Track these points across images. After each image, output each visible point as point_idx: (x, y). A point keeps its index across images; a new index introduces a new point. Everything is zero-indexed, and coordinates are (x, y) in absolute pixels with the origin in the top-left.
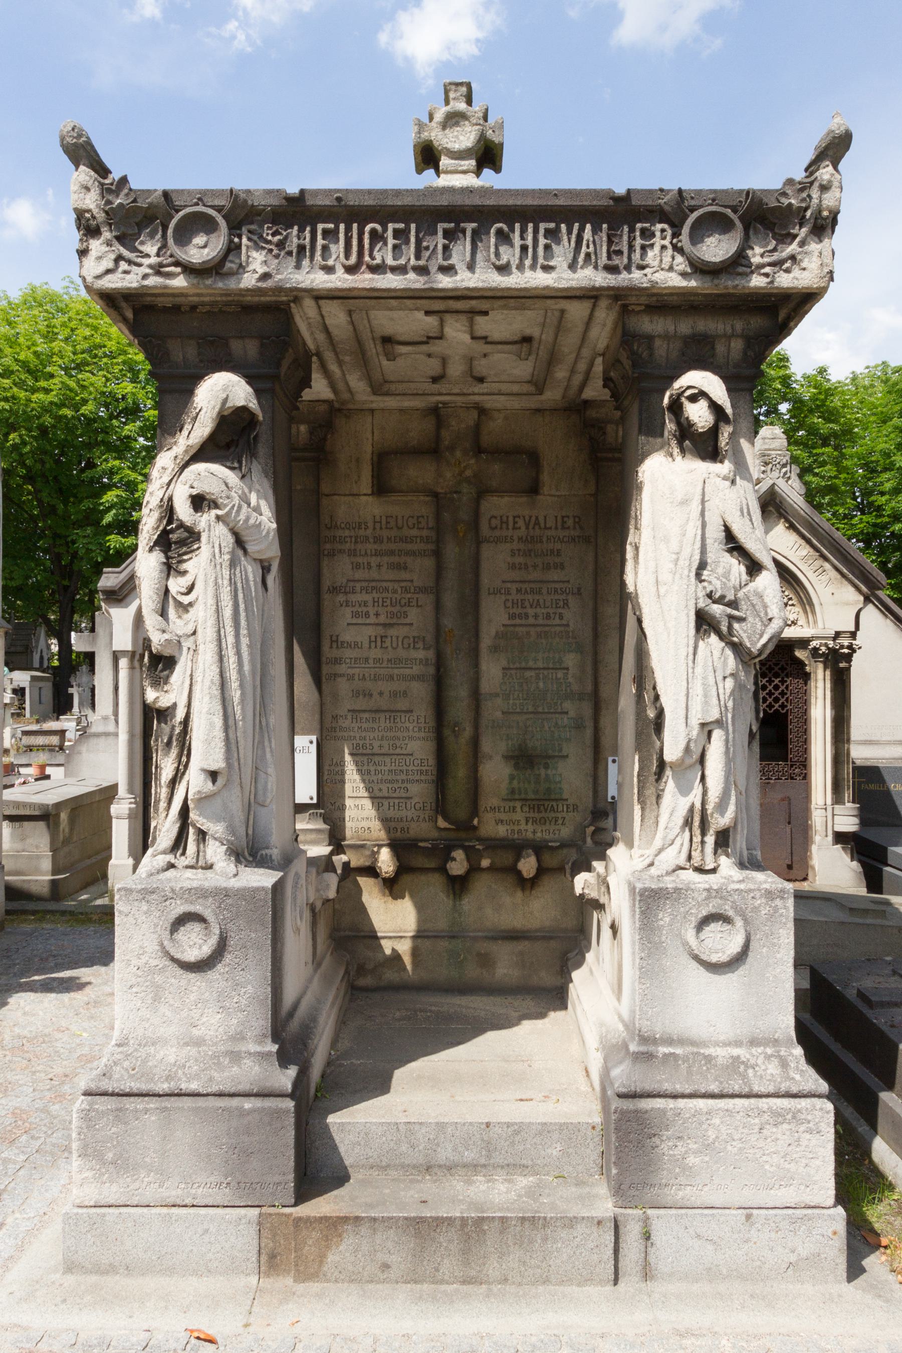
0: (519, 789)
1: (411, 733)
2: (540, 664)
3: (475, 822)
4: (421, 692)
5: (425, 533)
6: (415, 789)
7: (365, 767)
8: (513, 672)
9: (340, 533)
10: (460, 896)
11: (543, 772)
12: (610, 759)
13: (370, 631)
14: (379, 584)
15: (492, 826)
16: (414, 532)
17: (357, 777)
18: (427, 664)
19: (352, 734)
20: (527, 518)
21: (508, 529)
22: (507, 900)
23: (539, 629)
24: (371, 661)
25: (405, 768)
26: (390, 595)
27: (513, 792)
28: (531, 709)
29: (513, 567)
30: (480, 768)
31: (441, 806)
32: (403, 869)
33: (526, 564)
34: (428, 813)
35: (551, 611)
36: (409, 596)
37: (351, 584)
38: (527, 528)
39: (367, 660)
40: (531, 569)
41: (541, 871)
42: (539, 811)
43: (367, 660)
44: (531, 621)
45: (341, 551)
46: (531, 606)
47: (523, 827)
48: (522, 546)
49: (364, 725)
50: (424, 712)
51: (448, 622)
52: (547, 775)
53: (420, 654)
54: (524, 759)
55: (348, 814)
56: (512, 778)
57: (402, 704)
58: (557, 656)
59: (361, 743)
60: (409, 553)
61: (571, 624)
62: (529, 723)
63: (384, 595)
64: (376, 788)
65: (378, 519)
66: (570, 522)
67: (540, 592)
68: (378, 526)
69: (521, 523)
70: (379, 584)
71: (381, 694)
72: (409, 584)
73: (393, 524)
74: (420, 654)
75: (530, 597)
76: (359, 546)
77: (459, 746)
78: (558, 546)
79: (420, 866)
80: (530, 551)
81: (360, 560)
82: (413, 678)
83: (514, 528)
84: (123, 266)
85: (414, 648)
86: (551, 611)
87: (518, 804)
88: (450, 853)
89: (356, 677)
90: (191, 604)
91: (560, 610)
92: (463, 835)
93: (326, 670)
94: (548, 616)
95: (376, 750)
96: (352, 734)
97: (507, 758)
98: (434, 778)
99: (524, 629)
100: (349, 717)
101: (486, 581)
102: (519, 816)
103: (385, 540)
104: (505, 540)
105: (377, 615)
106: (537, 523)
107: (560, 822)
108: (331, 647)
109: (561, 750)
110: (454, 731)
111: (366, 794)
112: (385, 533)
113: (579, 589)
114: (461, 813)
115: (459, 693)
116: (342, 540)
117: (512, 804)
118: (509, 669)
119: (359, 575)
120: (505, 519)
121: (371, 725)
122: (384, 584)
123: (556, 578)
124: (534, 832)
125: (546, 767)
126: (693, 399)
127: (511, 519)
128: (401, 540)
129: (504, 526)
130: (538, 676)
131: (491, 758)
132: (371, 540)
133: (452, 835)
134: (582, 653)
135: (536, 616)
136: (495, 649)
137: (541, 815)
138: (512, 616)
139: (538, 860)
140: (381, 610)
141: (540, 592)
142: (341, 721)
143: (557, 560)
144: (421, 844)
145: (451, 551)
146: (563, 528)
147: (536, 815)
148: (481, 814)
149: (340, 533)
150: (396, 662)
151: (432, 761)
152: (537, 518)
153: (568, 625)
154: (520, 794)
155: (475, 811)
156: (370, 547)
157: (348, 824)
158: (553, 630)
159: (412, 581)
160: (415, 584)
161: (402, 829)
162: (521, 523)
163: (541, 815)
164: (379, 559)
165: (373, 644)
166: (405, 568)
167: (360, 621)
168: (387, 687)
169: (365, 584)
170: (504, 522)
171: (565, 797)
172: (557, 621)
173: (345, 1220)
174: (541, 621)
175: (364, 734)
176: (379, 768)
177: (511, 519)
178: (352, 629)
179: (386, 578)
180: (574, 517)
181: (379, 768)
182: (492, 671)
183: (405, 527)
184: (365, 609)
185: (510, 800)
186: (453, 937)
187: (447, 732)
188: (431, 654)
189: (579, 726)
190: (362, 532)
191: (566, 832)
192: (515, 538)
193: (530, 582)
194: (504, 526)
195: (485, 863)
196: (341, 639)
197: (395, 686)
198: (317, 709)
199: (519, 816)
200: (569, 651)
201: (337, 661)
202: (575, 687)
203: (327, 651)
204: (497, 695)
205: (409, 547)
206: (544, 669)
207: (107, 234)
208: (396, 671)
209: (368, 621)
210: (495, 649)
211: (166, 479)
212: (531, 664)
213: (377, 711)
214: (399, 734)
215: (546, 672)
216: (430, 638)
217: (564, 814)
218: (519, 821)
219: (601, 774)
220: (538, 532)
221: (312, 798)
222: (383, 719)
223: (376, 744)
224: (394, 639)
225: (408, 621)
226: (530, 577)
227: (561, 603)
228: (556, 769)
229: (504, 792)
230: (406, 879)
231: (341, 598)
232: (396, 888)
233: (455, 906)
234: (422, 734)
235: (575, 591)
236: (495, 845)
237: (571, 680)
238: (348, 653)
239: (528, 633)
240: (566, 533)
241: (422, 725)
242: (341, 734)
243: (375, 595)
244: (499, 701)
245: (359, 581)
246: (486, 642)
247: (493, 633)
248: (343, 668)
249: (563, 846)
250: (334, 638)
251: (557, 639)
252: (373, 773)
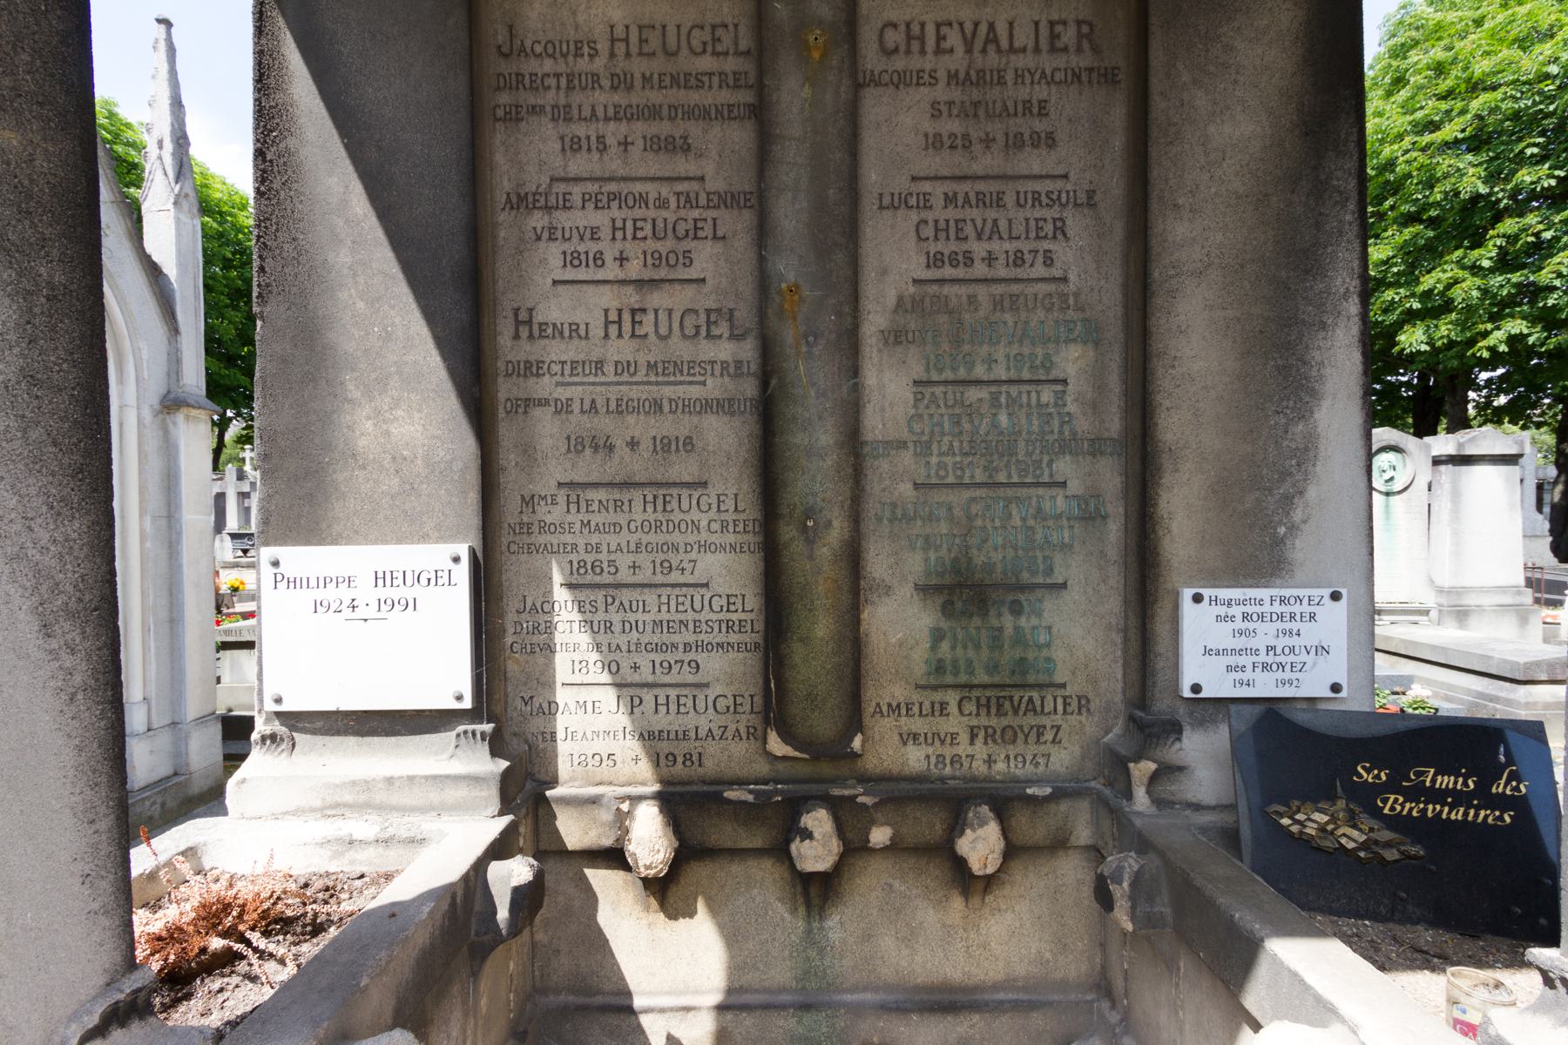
0: (955, 662)
1: (704, 535)
2: (1001, 372)
3: (857, 743)
4: (726, 439)
5: (731, 64)
6: (714, 665)
7: (601, 616)
8: (939, 390)
9: (530, 66)
10: (822, 909)
11: (1008, 622)
12: (1187, 594)
13: (607, 298)
14: (625, 188)
15: (893, 747)
16: (706, 63)
17: (584, 639)
18: (738, 375)
19: (568, 538)
20: (968, 27)
21: (923, 52)
22: (928, 916)
23: (998, 289)
24: (609, 368)
25: (690, 616)
26: (652, 213)
27: (939, 668)
28: (980, 476)
29: (935, 143)
30: (864, 616)
31: (775, 705)
32: (687, 853)
33: (966, 136)
34: (745, 720)
35: (1025, 246)
36: (696, 213)
37: (561, 188)
38: (969, 51)
39: (599, 365)
40: (977, 148)
41: (1012, 852)
42: (1000, 713)
43: (599, 365)
44: (980, 269)
45: (536, 110)
46: (979, 237)
47: (963, 748)
48: (956, 94)
49: (597, 519)
50: (732, 486)
51: (787, 268)
52: (1016, 628)
53: (724, 351)
54: (964, 592)
55: (562, 722)
56: (937, 636)
57: (683, 468)
58: (1040, 351)
59: (589, 559)
60: (691, 113)
61: (1072, 277)
62: (975, 509)
63: (639, 213)
64: (625, 665)
65: (619, 32)
66: (1068, 36)
67: (999, 203)
68: (620, 48)
69: (954, 39)
70: (625, 188)
71: (633, 444)
72: (695, 186)
73: (654, 43)
74: (724, 351)
75: (975, 213)
76: (577, 98)
77: (816, 566)
78: (1041, 92)
79: (729, 844)
80: (976, 104)
81: (580, 130)
82: (706, 406)
83: (938, 51)
85: (709, 336)
86: (1025, 246)
87: (952, 698)
88: (795, 817)
89: (576, 407)
91: (1046, 245)
92: (826, 769)
93: (505, 390)
94: (1018, 260)
95: (625, 576)
96: (568, 538)
97: (924, 590)
98: (758, 638)
99: (963, 290)
100: (562, 499)
101: (872, 177)
102: (954, 723)
103: (638, 83)
104: (919, 79)
105: (622, 259)
106: (992, 38)
107: (1049, 736)
108: (517, 337)
109: (1050, 571)
110: (804, 529)
111: (605, 678)
112: (639, 67)
113: (1091, 194)
114: (823, 724)
115: (814, 438)
116: (537, 84)
117: (938, 696)
118: (929, 383)
119: (579, 165)
120: (916, 29)
121: (611, 517)
122: (638, 188)
123: (1036, 169)
124: (990, 761)
125: (1017, 609)
127: (930, 30)
128: (675, 80)
129: (915, 45)
130: (995, 398)
131: (888, 590)
132: (606, 83)
133: (803, 770)
134: (1097, 344)
135: (990, 259)
136: (895, 337)
137: (1005, 722)
138: (935, 261)
139: (1005, 832)
140: (633, 249)
141: (999, 203)
142: (542, 509)
143: (1040, 126)
144: (731, 794)
145: (794, 97)
146: (1053, 49)
147: (994, 722)
148: (867, 720)
149: (530, 66)
150: (664, 369)
151: (753, 601)
152: (991, 26)
153: (1065, 280)
154: (956, 674)
155: (854, 720)
156: (602, 98)
157: (564, 748)
158: (1030, 290)
159: (702, 179)
160: (711, 185)
161: (688, 757)
162: (954, 39)
163: (1005, 722)
164: (623, 127)
165: (613, 329)
166: (686, 149)
167: (582, 274)
168: (644, 427)
169: (592, 188)
170: (914, 37)
171: (1059, 678)
172: (1039, 270)
174: (1002, 272)
175: (595, 539)
176: (632, 617)
177: (930, 30)
178: (564, 294)
179: (641, 172)
180: (1079, 23)
181: (632, 617)
182: (889, 388)
183: (685, 51)
184: (593, 247)
185: (935, 688)
186: (806, 1007)
187: (787, 532)
188: (748, 350)
189: (1091, 516)
190: (583, 64)
191: (1062, 759)
192: (941, 74)
193: (975, 178)
194: (915, 45)
195: (880, 836)
196: (539, 317)
197: (666, 426)
198: (473, 477)
199: (954, 723)
200: (1068, 341)
201: (532, 369)
202: (1083, 425)
203: (507, 346)
204: (902, 445)
205: (694, 97)
206: (1010, 382)
208: (668, 391)
209: (600, 275)
210: (895, 337)
212: (980, 371)
213: (627, 485)
214: (676, 538)
215: (1014, 390)
216: (745, 314)
217: (1058, 719)
218: (954, 736)
219: (1161, 628)
220: (993, 59)
221: (459, 698)
222: (638, 505)
223: (624, 561)
224: (662, 316)
225: (693, 273)
226: (977, 168)
227: (1049, 228)
228: (1039, 615)
229: (919, 669)
230: (699, 872)
231: (538, 220)
232: (675, 893)
233: (809, 932)
234: (731, 538)
235: (1082, 198)
236: (902, 793)
237: (1072, 407)
238: (557, 351)
239: (972, 299)
240: (1061, 61)
241: (730, 517)
242: (542, 539)
243: (615, 213)
244: (907, 458)
245: (577, 180)
246: (875, 321)
247: (891, 301)
248: (544, 387)
249: (1058, 795)
250: (523, 316)
251: (1041, 313)
252: (617, 628)
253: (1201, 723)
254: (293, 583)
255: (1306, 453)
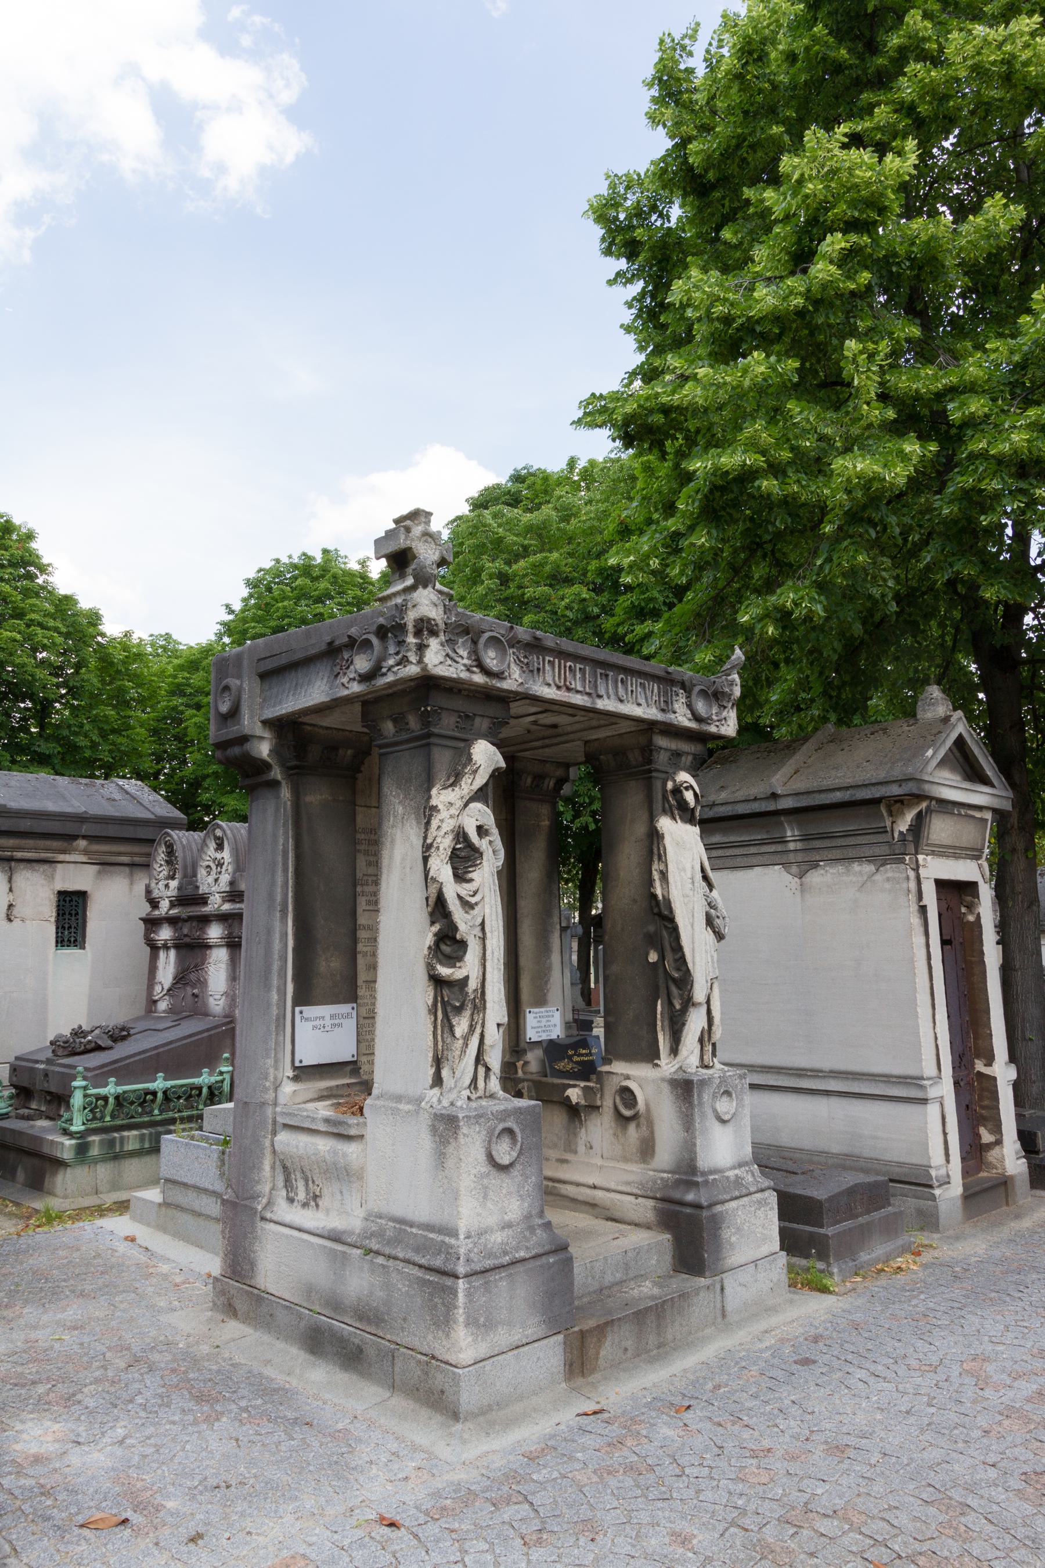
84: (449, 662)
90: (476, 904)
126: (687, 789)
173: (607, 1324)
207: (442, 637)
211: (454, 811)
253: (531, 1050)
254: (307, 1019)
255: (550, 968)
